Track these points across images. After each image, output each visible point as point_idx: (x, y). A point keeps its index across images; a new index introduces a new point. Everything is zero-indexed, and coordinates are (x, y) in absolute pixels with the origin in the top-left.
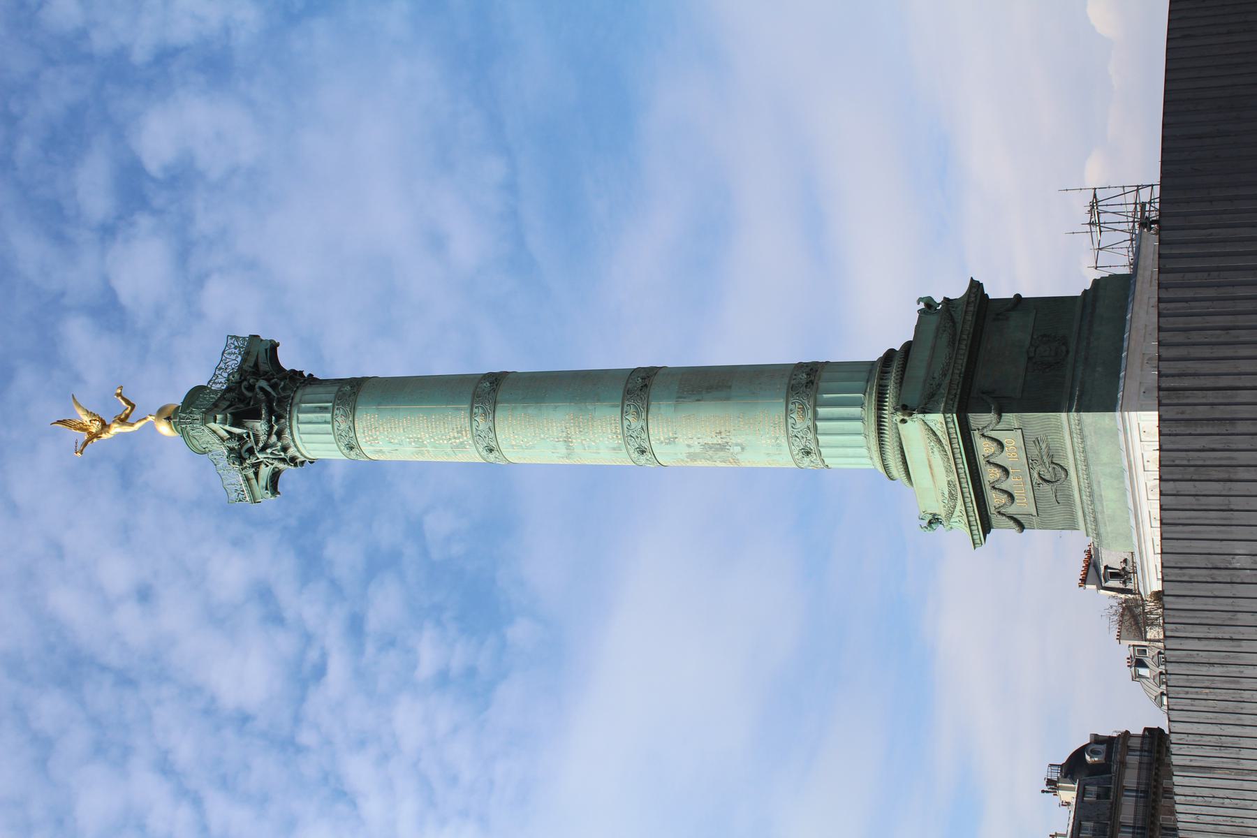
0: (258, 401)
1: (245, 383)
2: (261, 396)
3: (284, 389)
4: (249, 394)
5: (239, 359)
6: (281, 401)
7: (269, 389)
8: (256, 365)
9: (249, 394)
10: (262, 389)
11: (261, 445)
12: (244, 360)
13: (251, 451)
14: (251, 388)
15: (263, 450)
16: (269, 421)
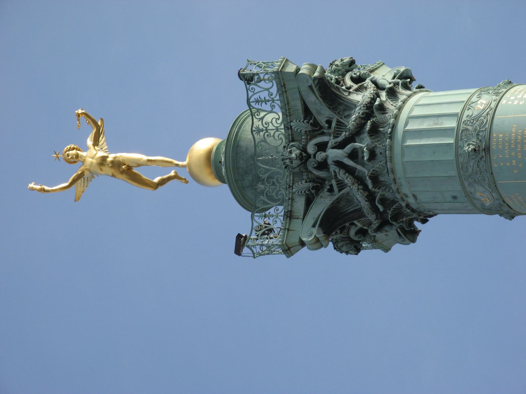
0: (341, 185)
1: (311, 164)
2: (342, 175)
3: (373, 155)
4: (322, 174)
5: (277, 109)
6: (375, 178)
7: (350, 163)
8: (307, 112)
9: (322, 174)
10: (339, 164)
11: (374, 226)
12: (287, 113)
13: (362, 232)
14: (323, 165)
15: (379, 229)
16: (375, 209)
